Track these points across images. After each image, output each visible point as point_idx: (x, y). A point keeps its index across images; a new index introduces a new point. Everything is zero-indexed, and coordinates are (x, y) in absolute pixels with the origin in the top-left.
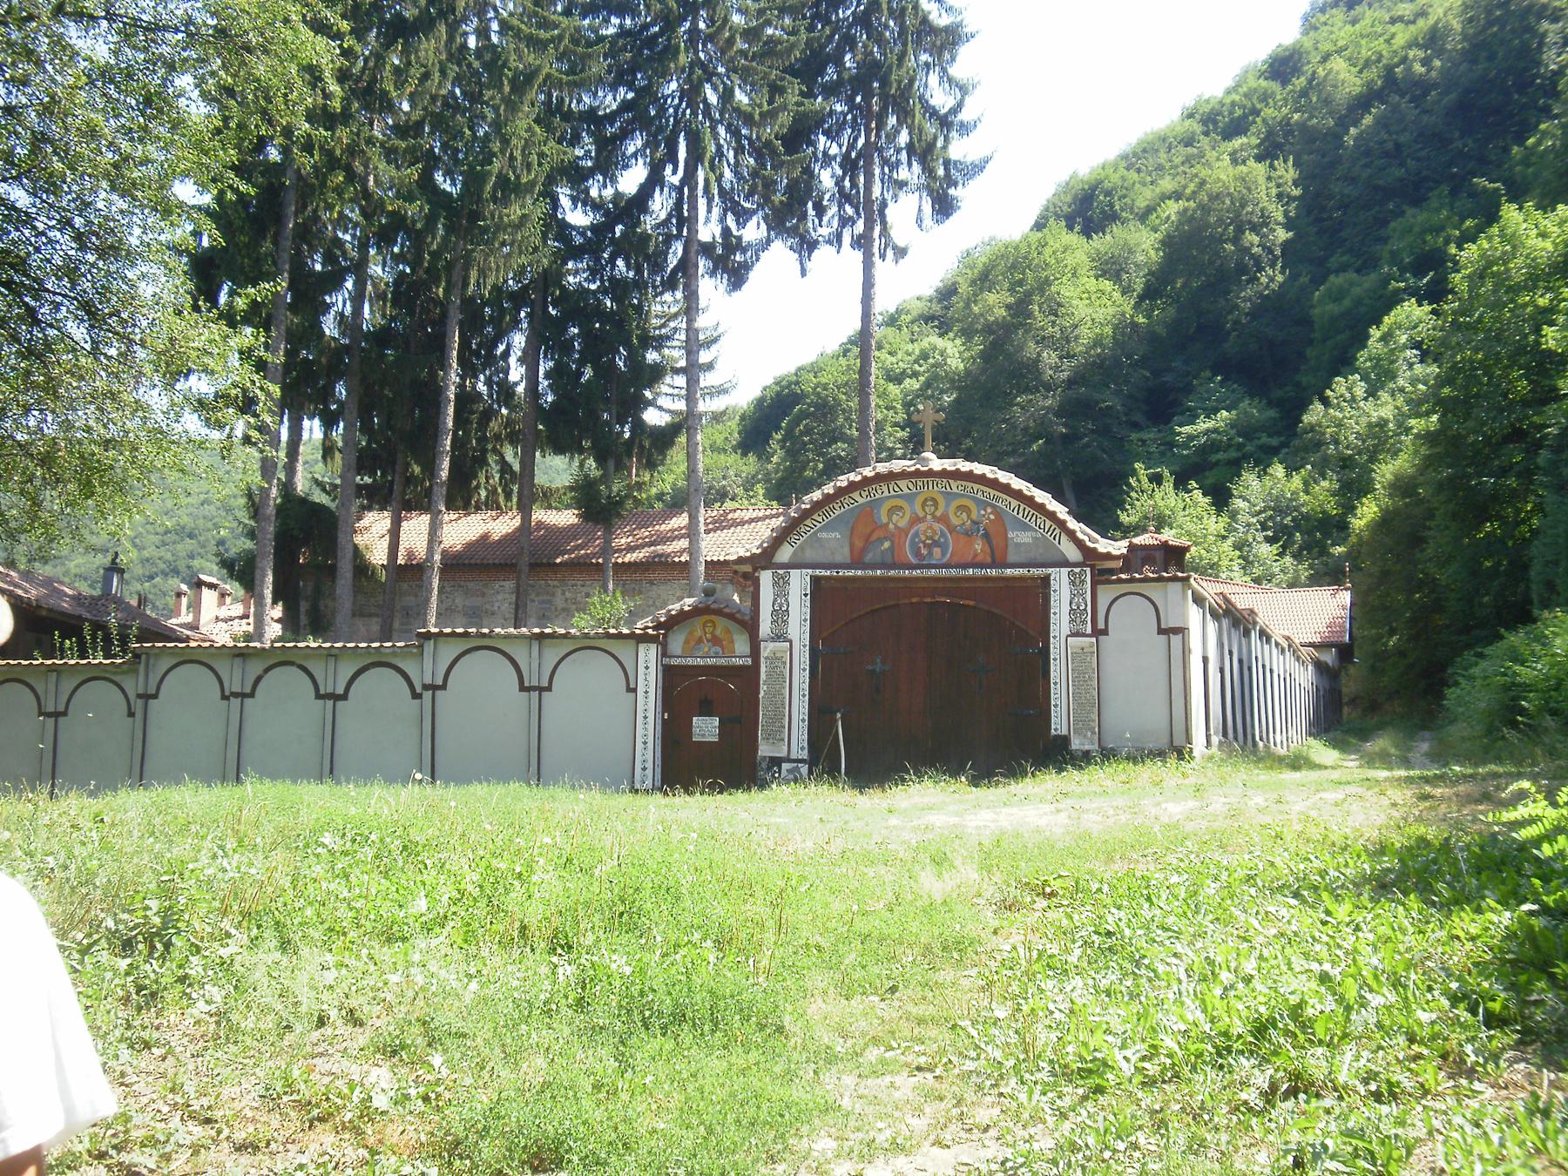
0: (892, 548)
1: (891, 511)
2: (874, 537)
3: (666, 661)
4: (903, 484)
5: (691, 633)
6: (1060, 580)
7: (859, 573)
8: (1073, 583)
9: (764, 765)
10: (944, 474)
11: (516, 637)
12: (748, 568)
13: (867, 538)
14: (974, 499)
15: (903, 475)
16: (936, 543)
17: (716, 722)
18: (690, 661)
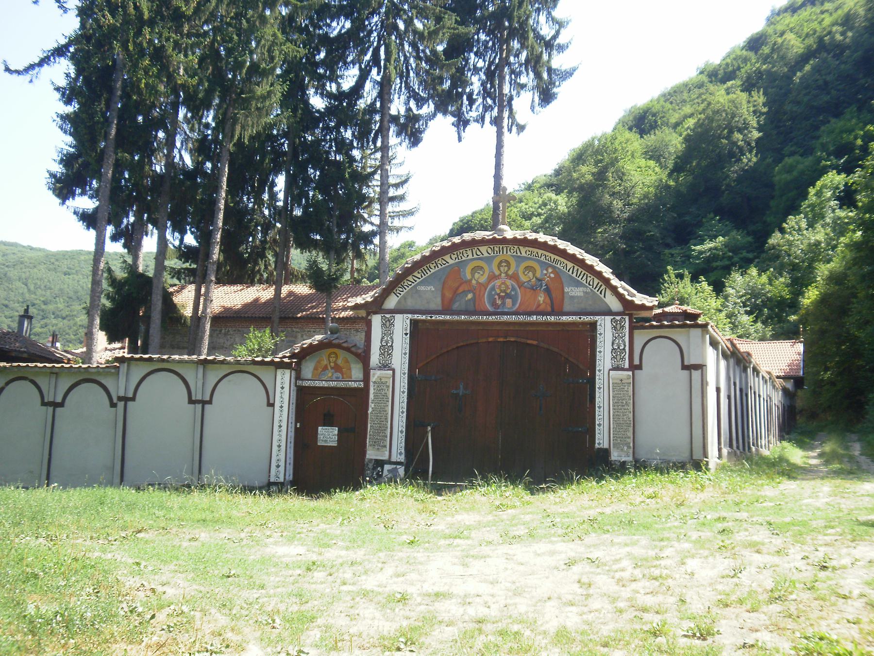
0: (474, 299)
2: (460, 290)
3: (299, 383)
4: (483, 249)
5: (319, 362)
6: (605, 324)
7: (448, 317)
8: (615, 328)
9: (371, 466)
10: (515, 241)
11: (187, 362)
12: (362, 313)
13: (455, 292)
14: (539, 262)
15: (483, 242)
16: (508, 296)
17: (335, 430)
18: (318, 384)
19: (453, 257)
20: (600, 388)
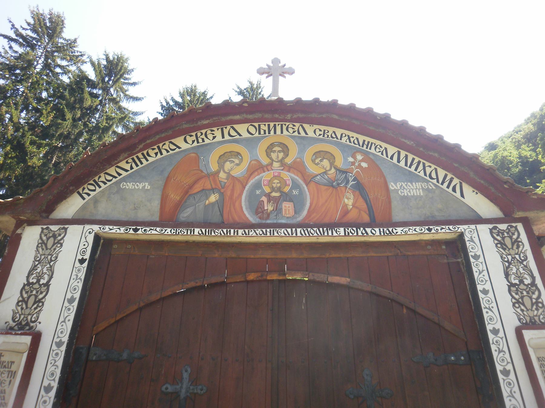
0: (221, 204)
1: (223, 158)
2: (198, 188)
8: (501, 244)
13: (187, 193)
16: (286, 197)
20: (506, 373)
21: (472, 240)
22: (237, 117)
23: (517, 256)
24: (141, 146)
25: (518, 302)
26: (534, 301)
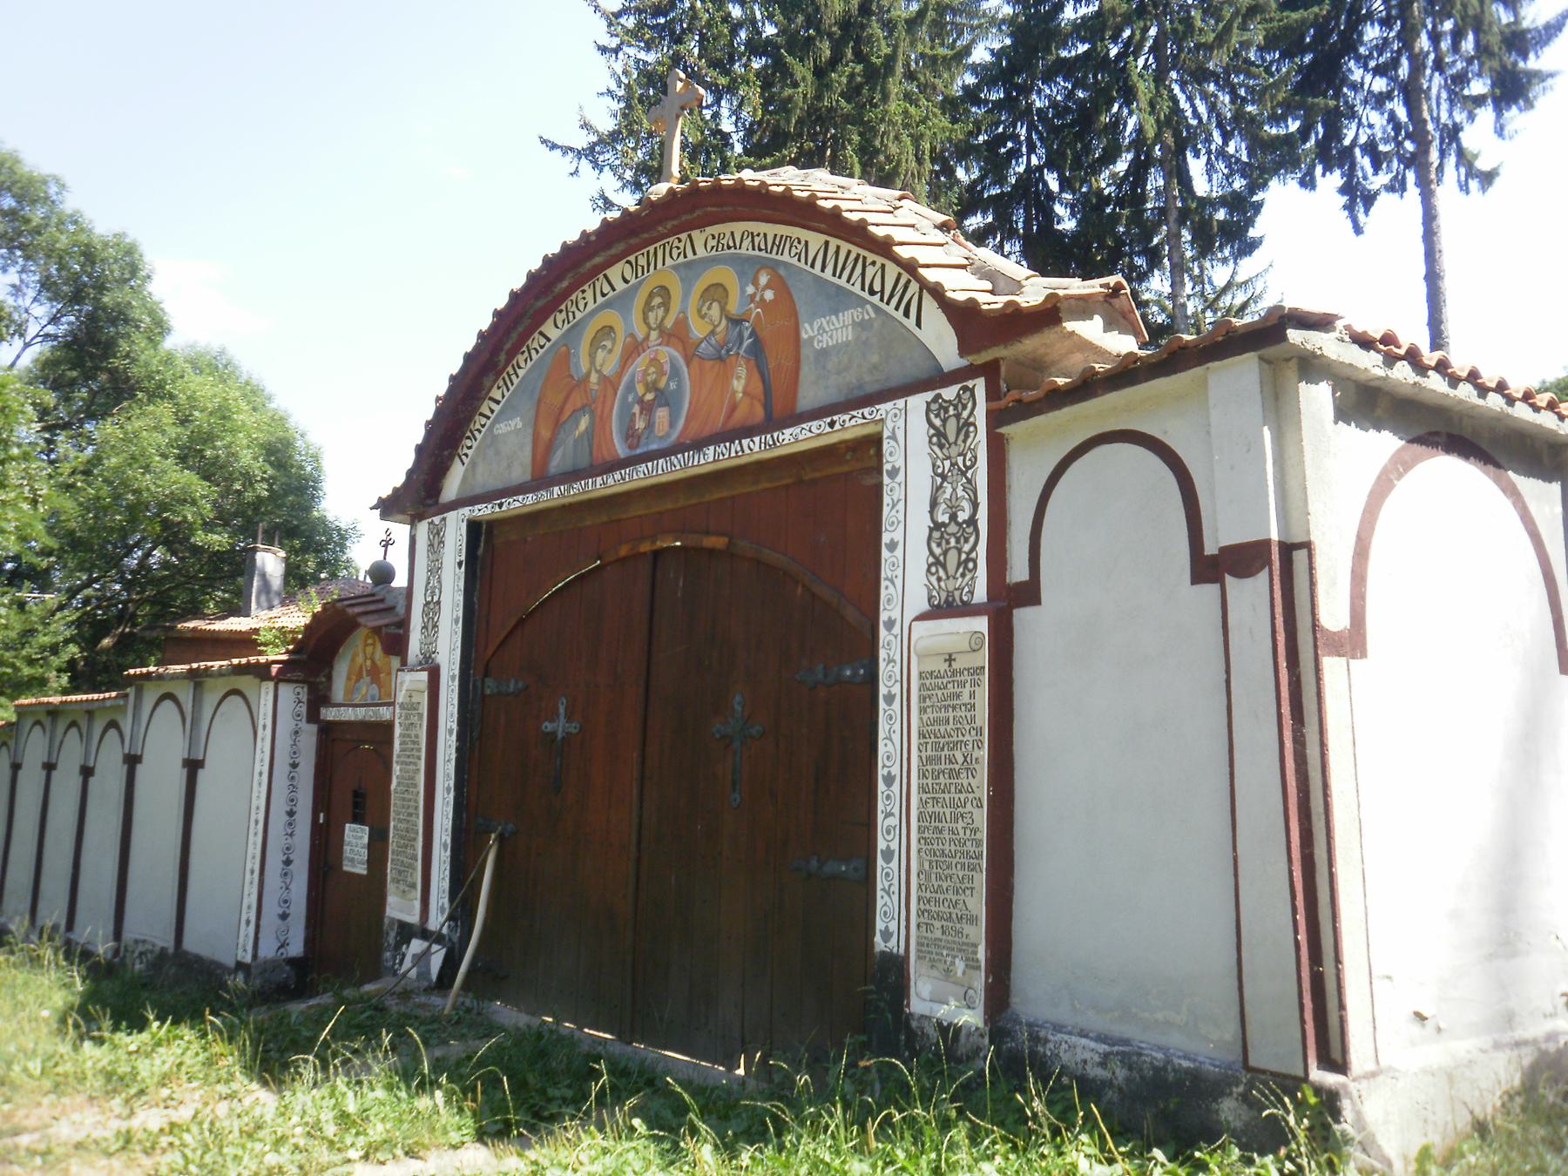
5: (353, 660)
6: (907, 428)
9: (392, 938)
19: (560, 317)
21: (893, 437)
22: (598, 260)
23: (960, 460)
24: (503, 357)
25: (937, 563)
26: (964, 556)
